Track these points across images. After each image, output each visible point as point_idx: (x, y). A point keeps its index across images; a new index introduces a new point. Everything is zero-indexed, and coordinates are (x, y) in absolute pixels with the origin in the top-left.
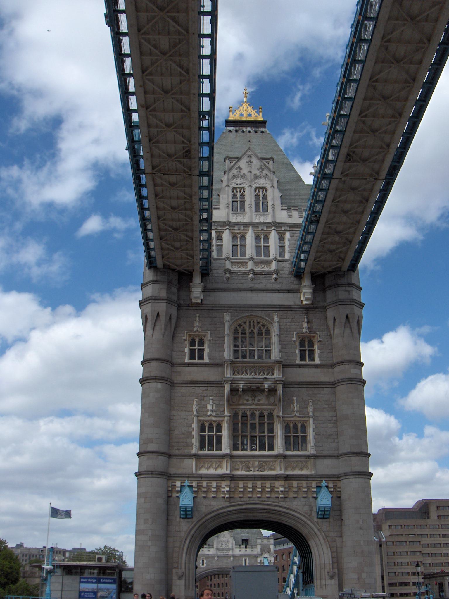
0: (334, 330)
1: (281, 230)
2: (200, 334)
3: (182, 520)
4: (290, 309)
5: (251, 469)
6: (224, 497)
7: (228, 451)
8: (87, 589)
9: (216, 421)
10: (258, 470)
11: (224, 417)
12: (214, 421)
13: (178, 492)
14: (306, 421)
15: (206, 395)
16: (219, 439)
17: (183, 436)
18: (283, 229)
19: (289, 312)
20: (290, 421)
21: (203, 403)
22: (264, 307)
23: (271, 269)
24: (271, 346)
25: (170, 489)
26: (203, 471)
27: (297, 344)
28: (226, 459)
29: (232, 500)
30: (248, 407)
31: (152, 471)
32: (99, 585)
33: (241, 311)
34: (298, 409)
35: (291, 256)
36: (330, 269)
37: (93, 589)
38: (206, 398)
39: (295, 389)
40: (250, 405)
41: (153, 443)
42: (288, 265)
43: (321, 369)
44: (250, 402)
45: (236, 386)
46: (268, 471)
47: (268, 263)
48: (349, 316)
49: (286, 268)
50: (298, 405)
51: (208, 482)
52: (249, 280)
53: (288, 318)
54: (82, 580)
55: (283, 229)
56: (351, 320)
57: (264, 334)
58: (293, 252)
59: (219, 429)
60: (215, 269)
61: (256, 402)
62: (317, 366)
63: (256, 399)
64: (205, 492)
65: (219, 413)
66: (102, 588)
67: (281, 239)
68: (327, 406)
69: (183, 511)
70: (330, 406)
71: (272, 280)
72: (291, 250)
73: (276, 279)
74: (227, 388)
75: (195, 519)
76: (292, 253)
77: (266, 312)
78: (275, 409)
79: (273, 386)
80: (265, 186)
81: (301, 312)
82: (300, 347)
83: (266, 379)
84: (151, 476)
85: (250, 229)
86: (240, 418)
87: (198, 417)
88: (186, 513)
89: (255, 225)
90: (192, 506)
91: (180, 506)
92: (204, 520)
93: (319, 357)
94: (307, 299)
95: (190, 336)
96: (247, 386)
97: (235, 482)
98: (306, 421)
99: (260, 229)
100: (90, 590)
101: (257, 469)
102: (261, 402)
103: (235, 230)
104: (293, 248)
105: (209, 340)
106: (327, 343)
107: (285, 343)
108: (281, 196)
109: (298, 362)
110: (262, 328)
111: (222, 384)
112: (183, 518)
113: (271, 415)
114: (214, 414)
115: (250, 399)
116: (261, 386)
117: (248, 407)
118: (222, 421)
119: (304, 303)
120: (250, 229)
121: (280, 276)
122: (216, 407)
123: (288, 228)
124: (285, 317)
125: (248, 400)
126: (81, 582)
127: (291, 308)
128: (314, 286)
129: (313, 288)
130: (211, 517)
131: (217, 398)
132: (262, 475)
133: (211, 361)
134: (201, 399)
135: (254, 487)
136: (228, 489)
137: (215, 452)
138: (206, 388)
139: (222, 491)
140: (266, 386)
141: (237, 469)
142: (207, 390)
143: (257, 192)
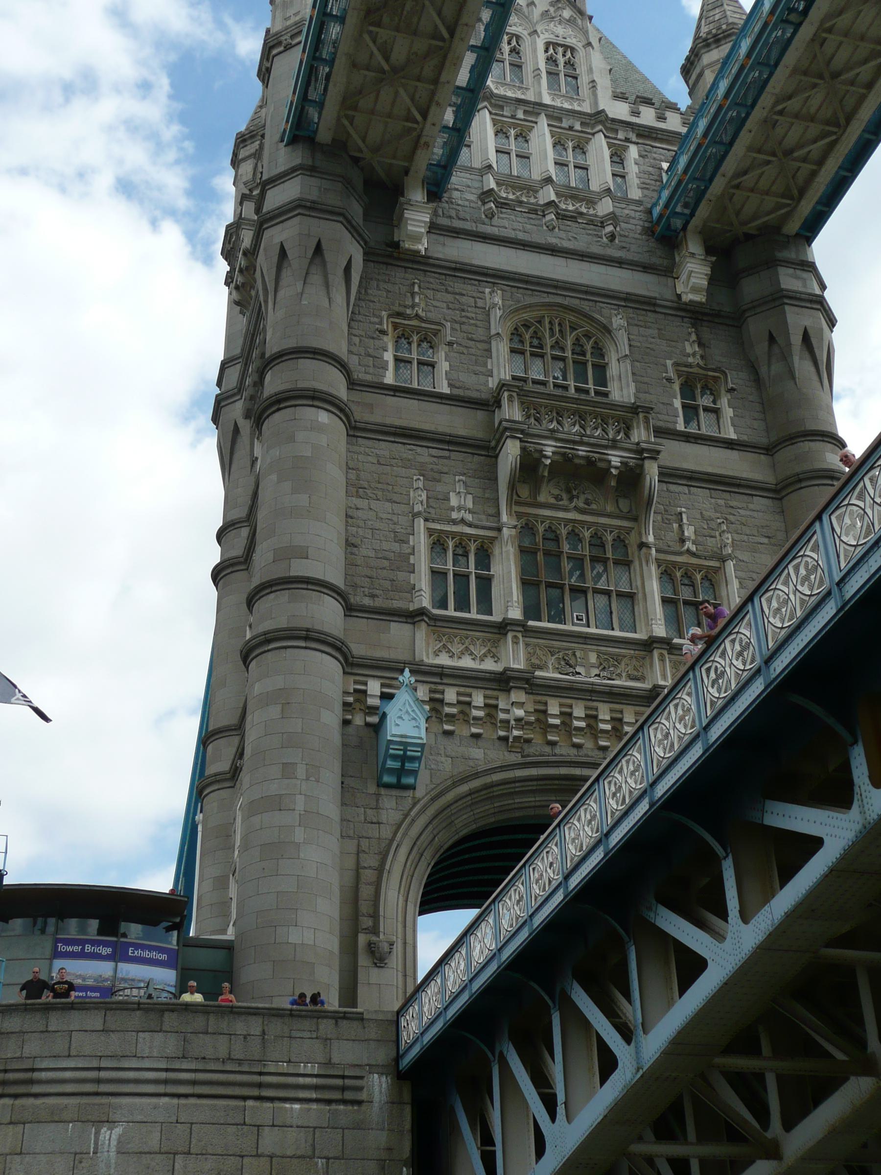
0: (769, 366)
1: (615, 139)
2: (423, 325)
3: (383, 791)
4: (652, 309)
5: (578, 669)
6: (505, 739)
7: (516, 613)
8: (80, 976)
9: (476, 538)
10: (598, 675)
11: (499, 530)
12: (470, 537)
13: (373, 710)
14: (717, 570)
15: (445, 469)
16: (485, 583)
17: (386, 563)
18: (621, 135)
19: (649, 314)
20: (674, 564)
21: (440, 488)
22: (586, 293)
23: (600, 214)
24: (609, 384)
25: (351, 699)
26: (444, 660)
27: (677, 387)
28: (510, 635)
29: (530, 750)
30: (561, 515)
31: (308, 630)
32: (120, 965)
33: (530, 292)
34: (693, 537)
35: (645, 196)
36: (752, 227)
37: (99, 979)
38: (446, 478)
39: (680, 488)
40: (566, 510)
41: (307, 558)
42: (639, 214)
43: (741, 453)
44: (565, 502)
45: (536, 450)
46: (626, 681)
47: (591, 202)
48: (811, 332)
49: (634, 218)
50: (692, 528)
51: (462, 690)
52: (545, 228)
53: (649, 328)
54: (61, 947)
55: (621, 135)
56: (814, 341)
57: (588, 356)
58: (647, 189)
59: (484, 557)
60: (457, 190)
61: (581, 505)
62: (730, 444)
63: (582, 498)
64: (451, 717)
65: (483, 517)
66: (130, 976)
67: (618, 157)
68: (766, 541)
69: (395, 757)
70: (772, 541)
71: (601, 238)
72: (644, 183)
73: (612, 237)
74: (511, 451)
75: (420, 792)
76: (646, 192)
77: (591, 304)
78: (633, 528)
79: (632, 463)
80: (571, 41)
81: (680, 319)
82: (682, 399)
83: (614, 445)
84: (302, 644)
85: (543, 122)
86: (539, 539)
87: (426, 520)
88: (403, 765)
89: (555, 115)
90: (425, 741)
91: (389, 738)
92: (450, 796)
93: (733, 425)
94: (695, 290)
95: (396, 326)
96: (564, 454)
97: (539, 698)
98: (717, 570)
99: (565, 124)
100: (90, 982)
101: (596, 671)
102: (594, 506)
103: (503, 116)
104: (649, 181)
105: (450, 344)
106: (751, 398)
107: (646, 380)
108: (610, 70)
109: (681, 426)
110: (584, 340)
111: (487, 448)
112: (388, 786)
113: (620, 542)
114: (469, 517)
115: (564, 496)
116: (601, 460)
117: (561, 515)
118: (492, 540)
119: (688, 297)
120: (543, 122)
121: (622, 232)
122: (473, 503)
123: (635, 135)
124: (643, 324)
125: (558, 498)
126: (57, 955)
127: (655, 305)
128: (714, 259)
129: (712, 263)
130: (471, 793)
131: (477, 480)
132: (613, 686)
133: (456, 392)
134: (432, 477)
135: (592, 718)
136: (520, 713)
137: (473, 615)
138: (446, 453)
139: (502, 721)
140: (615, 461)
141: (540, 668)
142: (448, 458)
143: (551, 51)
